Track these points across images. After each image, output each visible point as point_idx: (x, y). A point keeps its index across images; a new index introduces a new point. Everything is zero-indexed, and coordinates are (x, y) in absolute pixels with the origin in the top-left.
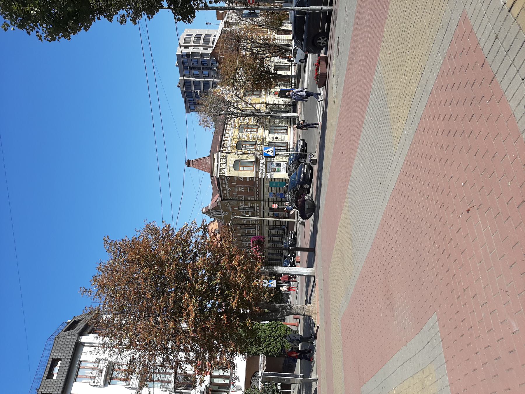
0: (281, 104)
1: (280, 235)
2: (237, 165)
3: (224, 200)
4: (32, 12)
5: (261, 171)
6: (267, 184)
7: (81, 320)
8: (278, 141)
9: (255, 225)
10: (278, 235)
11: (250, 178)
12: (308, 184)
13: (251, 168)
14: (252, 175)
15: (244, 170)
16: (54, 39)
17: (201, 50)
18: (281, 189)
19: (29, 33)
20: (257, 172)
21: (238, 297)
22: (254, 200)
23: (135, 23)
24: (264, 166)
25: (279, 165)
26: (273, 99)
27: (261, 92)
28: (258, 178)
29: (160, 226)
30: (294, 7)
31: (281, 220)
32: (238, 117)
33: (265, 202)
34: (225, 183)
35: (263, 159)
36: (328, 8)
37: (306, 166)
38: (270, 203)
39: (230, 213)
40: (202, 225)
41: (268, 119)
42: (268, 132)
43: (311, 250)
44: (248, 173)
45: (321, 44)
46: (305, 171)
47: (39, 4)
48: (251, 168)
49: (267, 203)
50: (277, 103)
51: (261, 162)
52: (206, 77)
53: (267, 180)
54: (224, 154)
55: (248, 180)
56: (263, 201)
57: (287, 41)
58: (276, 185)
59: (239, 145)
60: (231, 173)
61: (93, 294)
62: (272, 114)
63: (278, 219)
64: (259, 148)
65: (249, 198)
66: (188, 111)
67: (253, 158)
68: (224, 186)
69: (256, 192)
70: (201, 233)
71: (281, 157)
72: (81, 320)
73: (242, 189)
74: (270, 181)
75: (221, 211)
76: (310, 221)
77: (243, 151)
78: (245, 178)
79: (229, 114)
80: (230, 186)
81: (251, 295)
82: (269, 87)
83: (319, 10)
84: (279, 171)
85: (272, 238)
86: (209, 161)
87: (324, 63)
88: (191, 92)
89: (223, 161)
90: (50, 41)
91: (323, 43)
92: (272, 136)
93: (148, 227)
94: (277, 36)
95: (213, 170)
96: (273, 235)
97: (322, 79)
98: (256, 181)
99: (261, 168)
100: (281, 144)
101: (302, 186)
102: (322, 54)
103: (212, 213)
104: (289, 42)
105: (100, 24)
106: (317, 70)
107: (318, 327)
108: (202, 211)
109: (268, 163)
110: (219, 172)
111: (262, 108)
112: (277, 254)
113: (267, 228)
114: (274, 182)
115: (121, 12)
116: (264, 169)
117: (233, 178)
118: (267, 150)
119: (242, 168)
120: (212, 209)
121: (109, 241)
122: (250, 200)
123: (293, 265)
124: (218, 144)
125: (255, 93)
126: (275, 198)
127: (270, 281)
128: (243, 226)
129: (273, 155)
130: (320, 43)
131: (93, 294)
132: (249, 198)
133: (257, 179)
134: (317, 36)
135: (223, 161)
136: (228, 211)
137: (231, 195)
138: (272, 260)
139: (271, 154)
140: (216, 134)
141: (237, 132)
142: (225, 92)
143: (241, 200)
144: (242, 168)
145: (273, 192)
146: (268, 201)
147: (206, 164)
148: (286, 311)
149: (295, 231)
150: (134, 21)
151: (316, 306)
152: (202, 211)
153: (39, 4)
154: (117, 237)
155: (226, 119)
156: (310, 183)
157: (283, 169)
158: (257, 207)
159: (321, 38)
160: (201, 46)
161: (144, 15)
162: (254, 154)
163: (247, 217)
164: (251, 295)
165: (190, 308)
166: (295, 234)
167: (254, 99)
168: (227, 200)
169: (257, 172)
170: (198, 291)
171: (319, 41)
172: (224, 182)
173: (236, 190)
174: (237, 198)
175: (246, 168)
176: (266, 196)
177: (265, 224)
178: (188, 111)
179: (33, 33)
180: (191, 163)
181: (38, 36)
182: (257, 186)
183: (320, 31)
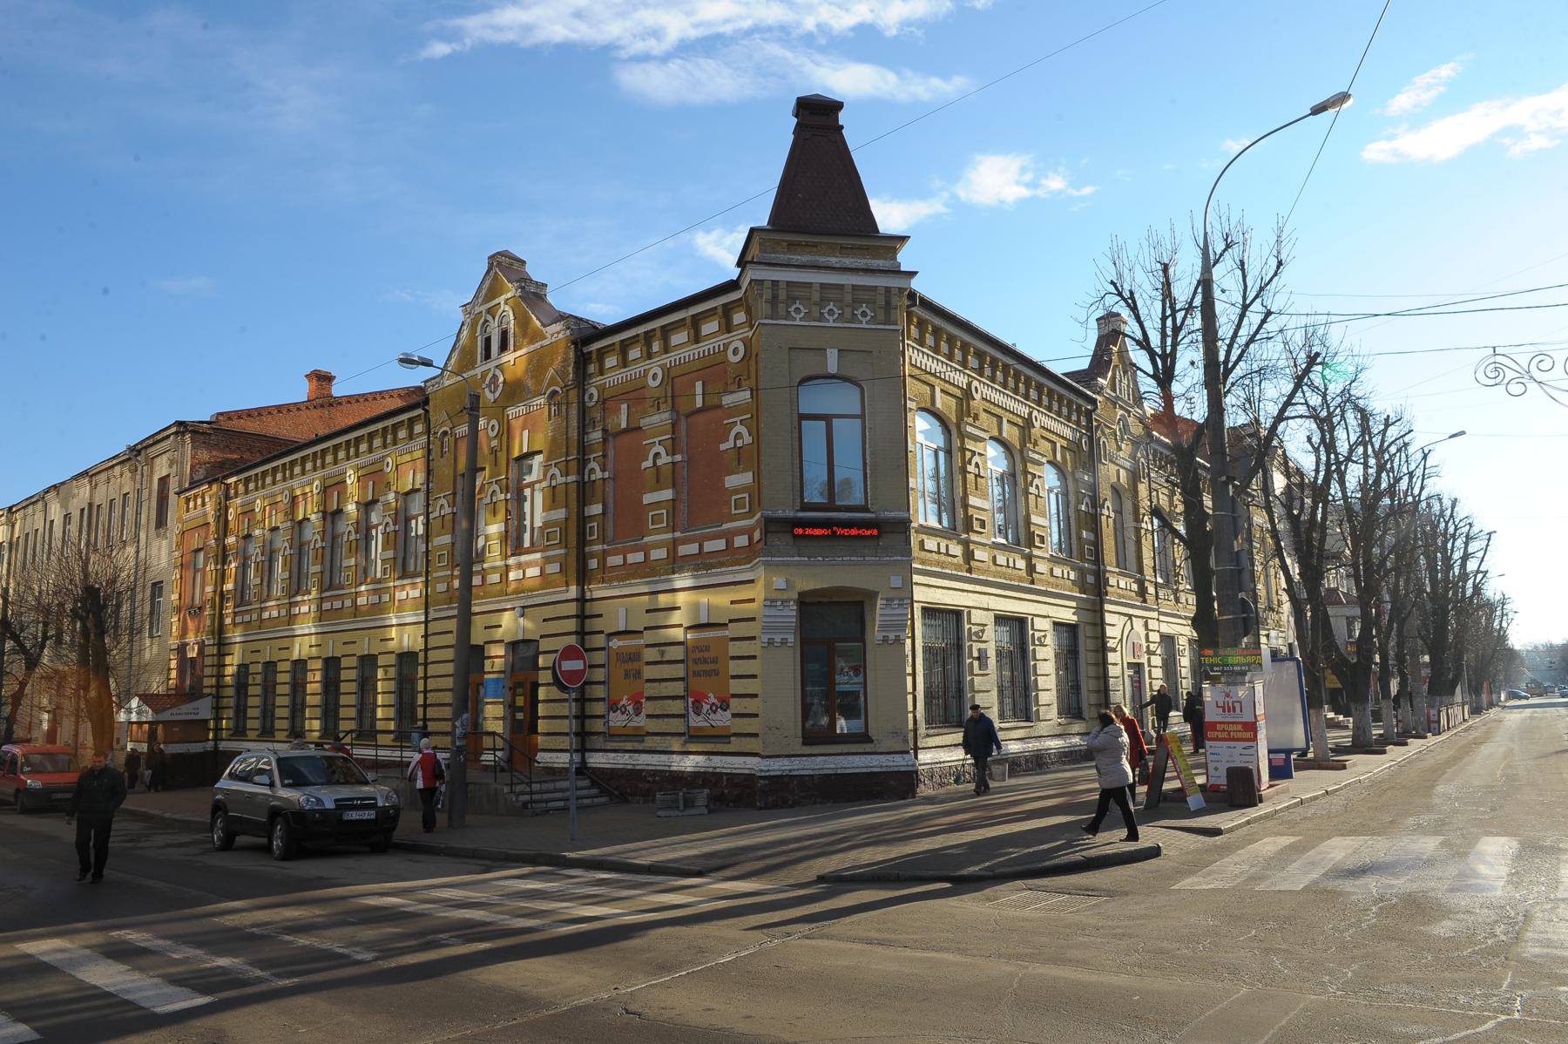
3: (582, 361)
22: (582, 542)
34: (697, 338)
55: (731, 481)
56: (582, 600)
68: (679, 338)
69: (646, 550)
73: (658, 454)
98: (729, 536)
122: (583, 520)
132: (596, 509)
143: (582, 463)
168: (582, 377)
174: (596, 436)
177: (433, 627)
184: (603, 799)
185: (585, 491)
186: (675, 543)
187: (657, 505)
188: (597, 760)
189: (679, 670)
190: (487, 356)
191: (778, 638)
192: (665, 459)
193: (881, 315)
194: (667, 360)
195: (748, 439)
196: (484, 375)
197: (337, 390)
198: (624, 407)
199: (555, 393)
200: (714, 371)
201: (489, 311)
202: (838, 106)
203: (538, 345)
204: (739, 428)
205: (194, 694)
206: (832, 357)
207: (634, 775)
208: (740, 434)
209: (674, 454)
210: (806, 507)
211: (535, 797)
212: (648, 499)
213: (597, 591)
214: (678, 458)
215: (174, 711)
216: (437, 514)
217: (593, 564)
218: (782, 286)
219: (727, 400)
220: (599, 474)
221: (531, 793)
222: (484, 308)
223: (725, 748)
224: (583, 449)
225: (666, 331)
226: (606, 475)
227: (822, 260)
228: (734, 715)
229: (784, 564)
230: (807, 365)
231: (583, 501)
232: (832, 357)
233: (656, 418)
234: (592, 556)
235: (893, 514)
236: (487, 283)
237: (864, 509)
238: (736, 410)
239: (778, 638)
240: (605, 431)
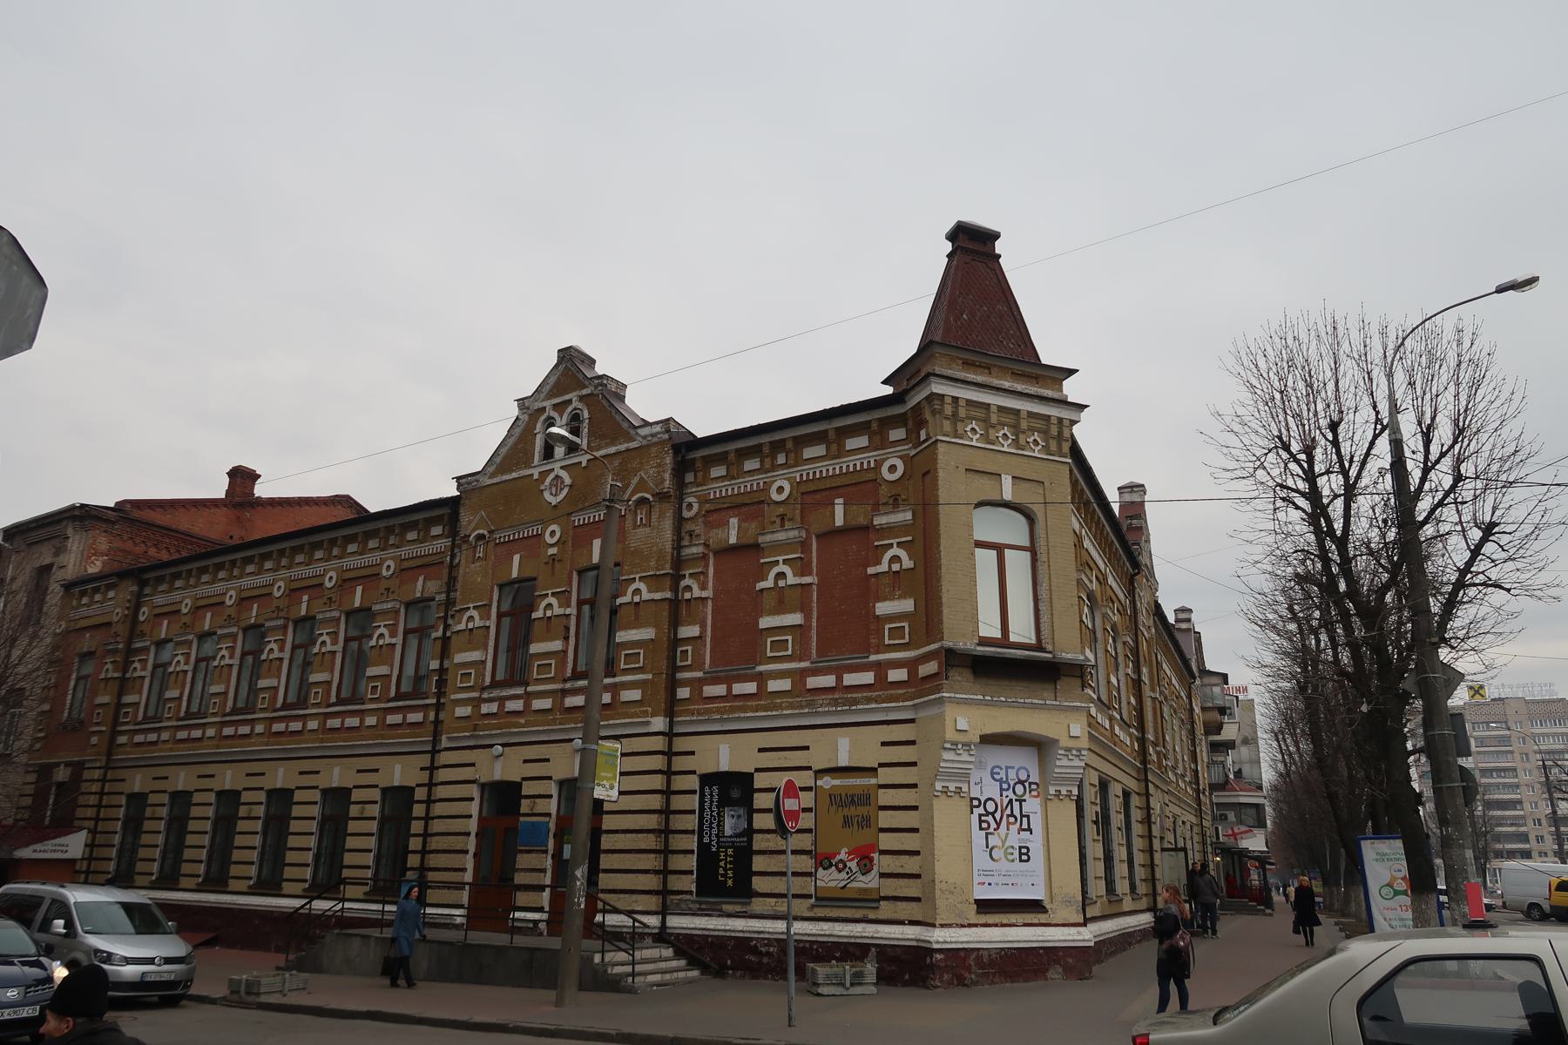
3: (681, 468)
6: (844, 749)
22: (674, 669)
33: (659, 743)
34: (842, 453)
48: (989, 627)
49: (657, 762)
55: (883, 608)
56: (670, 735)
73: (782, 573)
80: (814, 496)
98: (880, 668)
113: (400, 773)
122: (675, 642)
132: (689, 631)
137: (716, 512)
138: (134, 824)
143: (677, 578)
168: (680, 485)
184: (695, 973)
186: (804, 673)
188: (675, 922)
191: (952, 787)
192: (791, 579)
193: (1053, 446)
194: (797, 473)
195: (907, 563)
196: (544, 474)
197: (262, 490)
198: (734, 521)
199: (643, 501)
200: (863, 487)
201: (555, 407)
202: (996, 236)
203: (623, 447)
204: (895, 551)
205: (64, 825)
206: (1007, 481)
207: (743, 944)
208: (897, 557)
209: (803, 575)
210: (984, 641)
211: (638, 968)
212: (765, 622)
213: (684, 723)
214: (807, 580)
215: (38, 847)
216: (462, 626)
217: (683, 693)
218: (962, 403)
220: (697, 592)
221: (633, 963)
222: (548, 404)
223: (872, 916)
226: (704, 594)
227: (996, 382)
228: (882, 875)
229: (966, 702)
230: (985, 489)
231: (675, 623)
232: (1007, 481)
233: (781, 536)
234: (685, 683)
235: (1069, 656)
236: (552, 380)
237: (1039, 647)
238: (890, 530)
239: (952, 787)
240: (706, 545)
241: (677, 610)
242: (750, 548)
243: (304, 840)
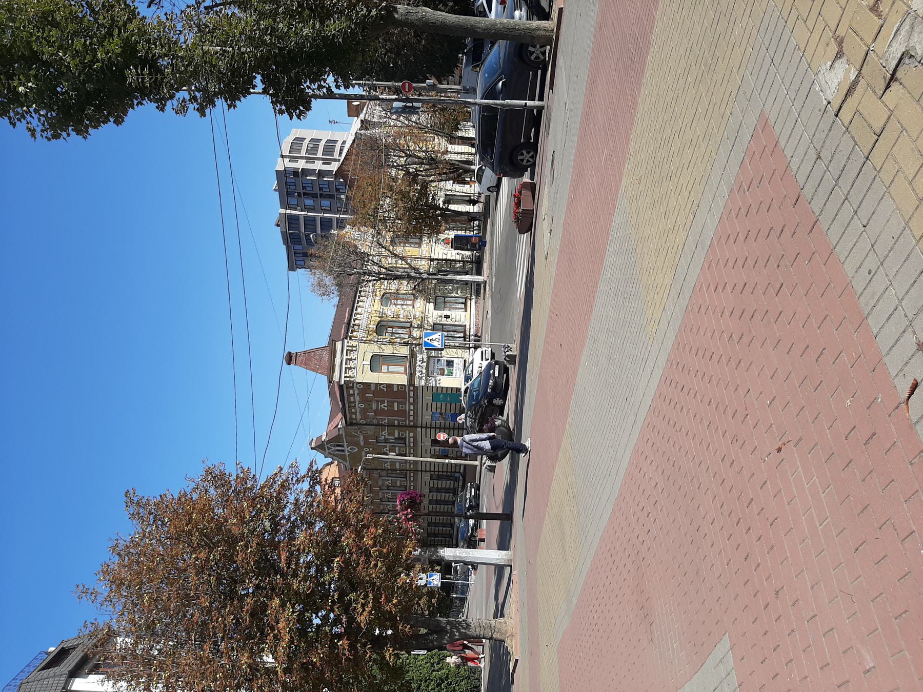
0: (455, 261)
1: (449, 489)
2: (376, 362)
3: (351, 424)
4: (21, 89)
5: (418, 374)
6: (428, 398)
7: (74, 648)
8: (449, 322)
9: (405, 471)
10: (447, 490)
11: (398, 385)
12: (500, 398)
13: (402, 369)
14: (403, 380)
15: (389, 372)
16: (56, 136)
17: (318, 166)
18: (453, 406)
19: (14, 125)
20: (411, 376)
21: (371, 605)
22: (405, 426)
23: (203, 114)
24: (425, 364)
25: (450, 363)
26: (441, 252)
27: (421, 238)
28: (413, 385)
29: (232, 471)
30: (478, 101)
31: (453, 461)
32: (380, 279)
33: (424, 430)
34: (353, 395)
35: (422, 353)
36: (537, 103)
37: (497, 367)
38: (433, 430)
39: (361, 449)
40: (309, 470)
41: (434, 284)
42: (432, 305)
43: (506, 518)
44: (396, 377)
45: (525, 162)
46: (496, 375)
47: (35, 76)
48: (402, 369)
49: (428, 430)
50: (449, 257)
51: (419, 357)
52: (325, 211)
53: (430, 389)
54: (354, 343)
55: (395, 389)
56: (422, 427)
57: (466, 157)
58: (445, 400)
59: (381, 328)
60: (364, 375)
61: (100, 598)
62: (439, 277)
63: (447, 461)
64: (416, 333)
65: (396, 422)
66: (292, 267)
67: (405, 351)
69: (410, 410)
70: (305, 486)
71: (455, 350)
72: (74, 648)
73: (384, 406)
74: (435, 391)
75: (346, 444)
76: (504, 464)
77: (388, 337)
78: (389, 386)
79: (364, 274)
80: (363, 400)
81: (395, 601)
82: (435, 230)
83: (522, 106)
84: (450, 374)
85: (435, 496)
86: (326, 356)
87: (530, 194)
88: (299, 235)
89: (352, 356)
90: (49, 139)
91: (528, 161)
92: (439, 313)
93: (209, 472)
94: (451, 148)
95: (334, 371)
96: (438, 490)
97: (525, 221)
98: (410, 391)
99: (418, 369)
100: (454, 328)
101: (490, 402)
102: (526, 179)
103: (329, 449)
104: (471, 158)
105: (143, 113)
106: (518, 204)
107: (517, 661)
108: (310, 444)
109: (431, 360)
110: (343, 375)
111: (423, 265)
112: (444, 525)
113: (427, 477)
114: (441, 394)
115: (183, 94)
116: (424, 371)
117: (368, 385)
118: (430, 338)
119: (384, 368)
120: (329, 442)
121: (136, 499)
122: (399, 426)
123: (472, 543)
124: (344, 327)
125: (411, 240)
126: (442, 422)
127: (431, 576)
128: (384, 473)
129: (440, 347)
130: (522, 160)
131: (100, 598)
132: (396, 422)
133: (412, 388)
134: (518, 148)
135: (352, 356)
136: (357, 444)
138: (435, 535)
139: (437, 344)
140: (340, 307)
141: (377, 306)
142: (359, 237)
143: (382, 425)
144: (384, 368)
145: (439, 411)
146: (431, 428)
147: (320, 360)
148: (458, 630)
149: (477, 482)
150: (202, 111)
151: (513, 621)
152: (310, 444)
153: (35, 76)
154: (150, 492)
155: (359, 283)
156: (504, 397)
157: (458, 372)
158: (410, 437)
159: (524, 152)
160: (318, 159)
161: (220, 102)
162: (406, 344)
163: (392, 456)
164: (395, 601)
165: (281, 625)
166: (478, 488)
167: (410, 250)
168: (356, 424)
169: (411, 376)
170: (297, 593)
171: (520, 157)
172: (351, 392)
173: (374, 406)
174: (375, 421)
175: (392, 368)
176: (427, 417)
178: (292, 267)
179: (22, 126)
180: (294, 359)
181: (29, 129)
182: (412, 400)
183: (522, 140)
185: (391, 425)
187: (398, 407)
189: (444, 404)
190: (343, 451)
202: (290, 353)
213: (419, 424)
219: (373, 389)
224: (378, 425)
225: (349, 402)
230: (367, 368)
241: (391, 425)
242: (375, 412)
243: (443, 496)
